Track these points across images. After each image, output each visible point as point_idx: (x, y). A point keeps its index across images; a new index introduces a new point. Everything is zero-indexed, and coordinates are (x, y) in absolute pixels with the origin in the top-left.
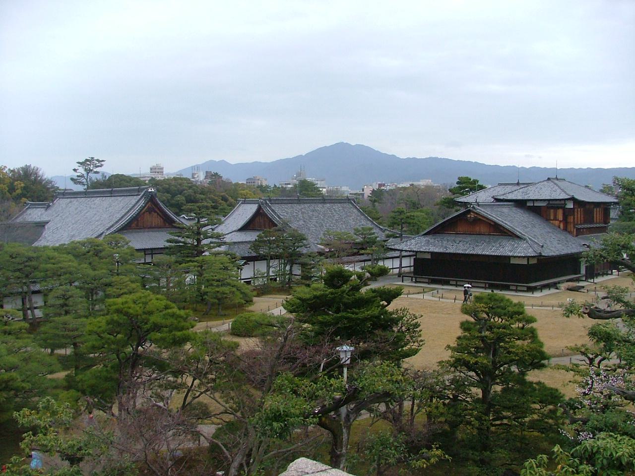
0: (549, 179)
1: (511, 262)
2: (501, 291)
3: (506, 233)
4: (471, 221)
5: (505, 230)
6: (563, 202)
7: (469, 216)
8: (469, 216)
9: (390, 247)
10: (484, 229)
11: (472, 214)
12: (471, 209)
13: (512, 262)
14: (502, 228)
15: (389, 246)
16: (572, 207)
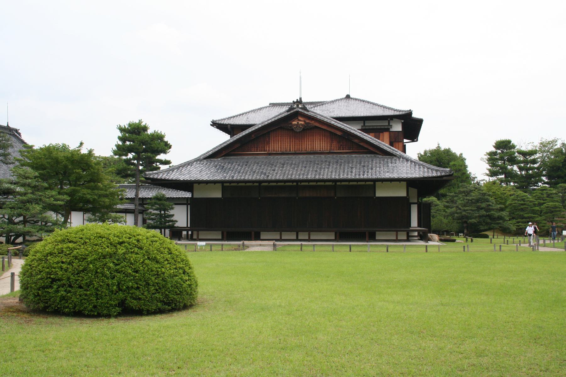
0: (348, 97)
1: (378, 195)
2: (367, 242)
3: (368, 149)
4: (298, 130)
5: (362, 144)
6: (385, 123)
7: (294, 123)
8: (294, 123)
9: (151, 177)
10: (320, 144)
11: (300, 118)
12: (300, 110)
13: (380, 193)
14: (356, 141)
15: (150, 174)
16: (401, 130)
